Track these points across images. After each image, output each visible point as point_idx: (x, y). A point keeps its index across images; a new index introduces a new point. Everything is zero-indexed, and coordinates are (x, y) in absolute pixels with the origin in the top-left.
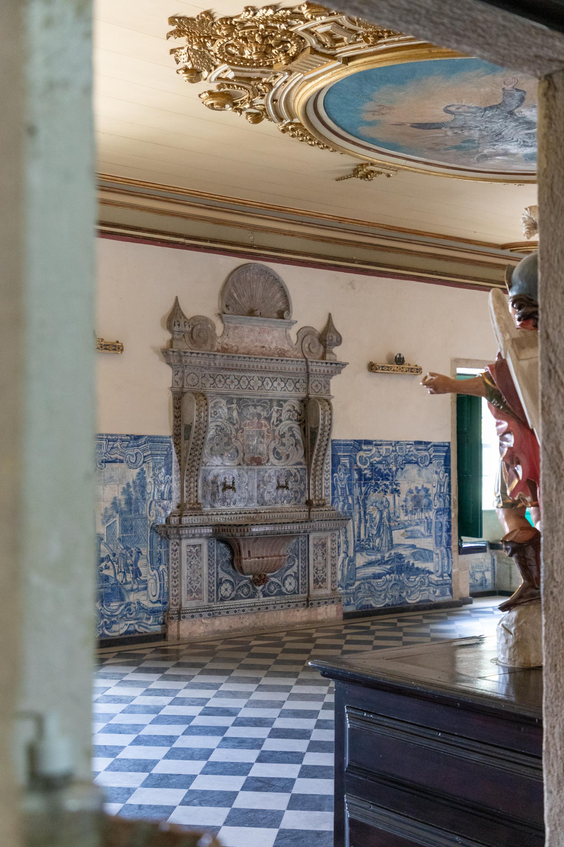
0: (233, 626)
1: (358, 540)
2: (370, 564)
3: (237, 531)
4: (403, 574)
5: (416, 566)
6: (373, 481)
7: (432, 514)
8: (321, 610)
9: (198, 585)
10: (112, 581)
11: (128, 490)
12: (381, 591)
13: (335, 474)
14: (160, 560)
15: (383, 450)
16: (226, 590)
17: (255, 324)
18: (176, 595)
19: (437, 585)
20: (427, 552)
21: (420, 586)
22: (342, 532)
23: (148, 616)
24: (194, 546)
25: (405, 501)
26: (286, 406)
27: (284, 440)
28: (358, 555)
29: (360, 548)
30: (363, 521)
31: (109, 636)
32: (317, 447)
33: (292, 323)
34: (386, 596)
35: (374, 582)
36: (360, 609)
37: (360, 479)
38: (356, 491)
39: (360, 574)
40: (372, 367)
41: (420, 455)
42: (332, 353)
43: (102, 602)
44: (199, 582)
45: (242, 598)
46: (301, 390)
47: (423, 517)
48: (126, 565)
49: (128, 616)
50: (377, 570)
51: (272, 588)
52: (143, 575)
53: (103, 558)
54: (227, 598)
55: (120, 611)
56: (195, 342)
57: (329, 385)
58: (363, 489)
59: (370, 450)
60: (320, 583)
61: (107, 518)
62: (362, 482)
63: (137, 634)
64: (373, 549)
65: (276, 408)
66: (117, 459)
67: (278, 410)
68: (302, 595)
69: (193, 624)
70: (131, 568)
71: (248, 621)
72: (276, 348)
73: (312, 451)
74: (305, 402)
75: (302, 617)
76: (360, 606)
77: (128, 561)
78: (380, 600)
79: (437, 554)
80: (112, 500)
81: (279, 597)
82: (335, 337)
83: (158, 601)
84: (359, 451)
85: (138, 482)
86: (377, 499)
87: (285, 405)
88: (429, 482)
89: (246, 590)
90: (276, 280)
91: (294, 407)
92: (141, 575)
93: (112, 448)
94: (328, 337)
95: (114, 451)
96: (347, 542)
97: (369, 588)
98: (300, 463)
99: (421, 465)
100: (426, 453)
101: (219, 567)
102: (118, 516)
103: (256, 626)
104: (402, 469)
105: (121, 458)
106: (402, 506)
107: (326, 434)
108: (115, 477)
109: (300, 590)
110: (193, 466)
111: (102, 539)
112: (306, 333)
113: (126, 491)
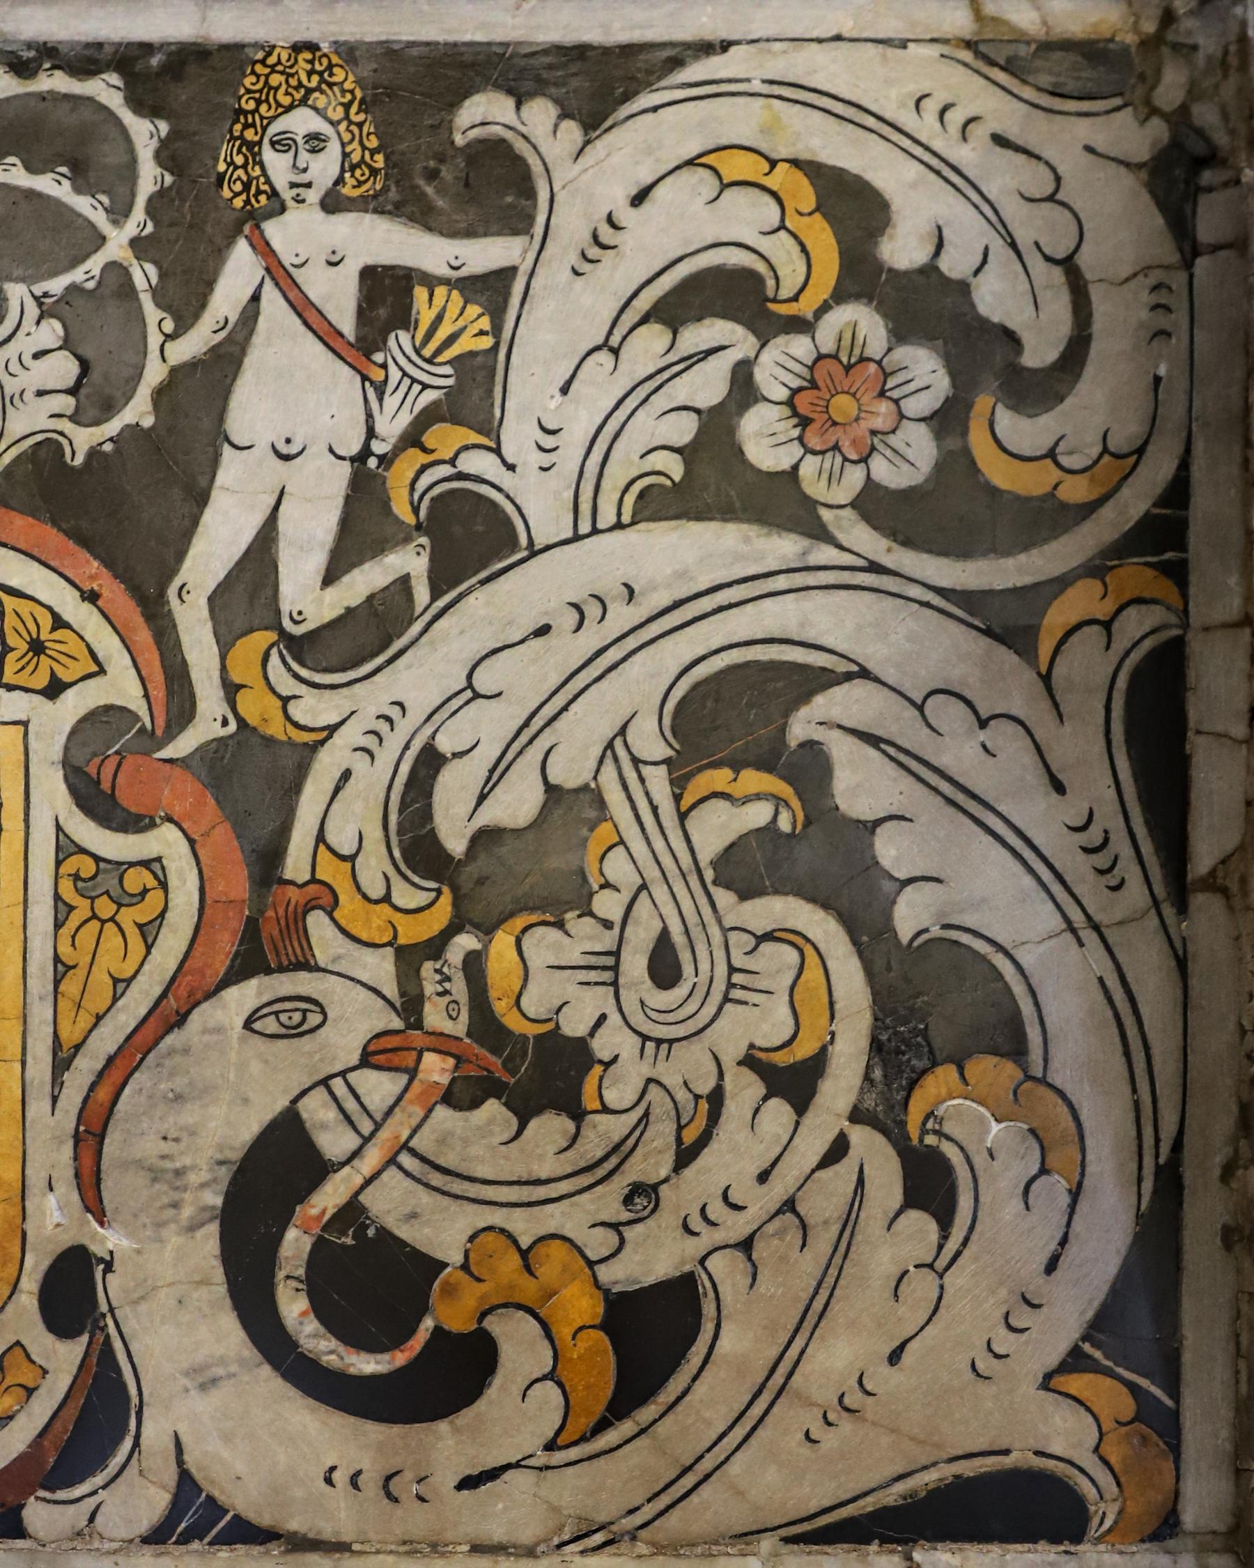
26: (629, 201)
65: (331, 247)
67: (387, 293)
87: (584, 175)
91: (851, 206)
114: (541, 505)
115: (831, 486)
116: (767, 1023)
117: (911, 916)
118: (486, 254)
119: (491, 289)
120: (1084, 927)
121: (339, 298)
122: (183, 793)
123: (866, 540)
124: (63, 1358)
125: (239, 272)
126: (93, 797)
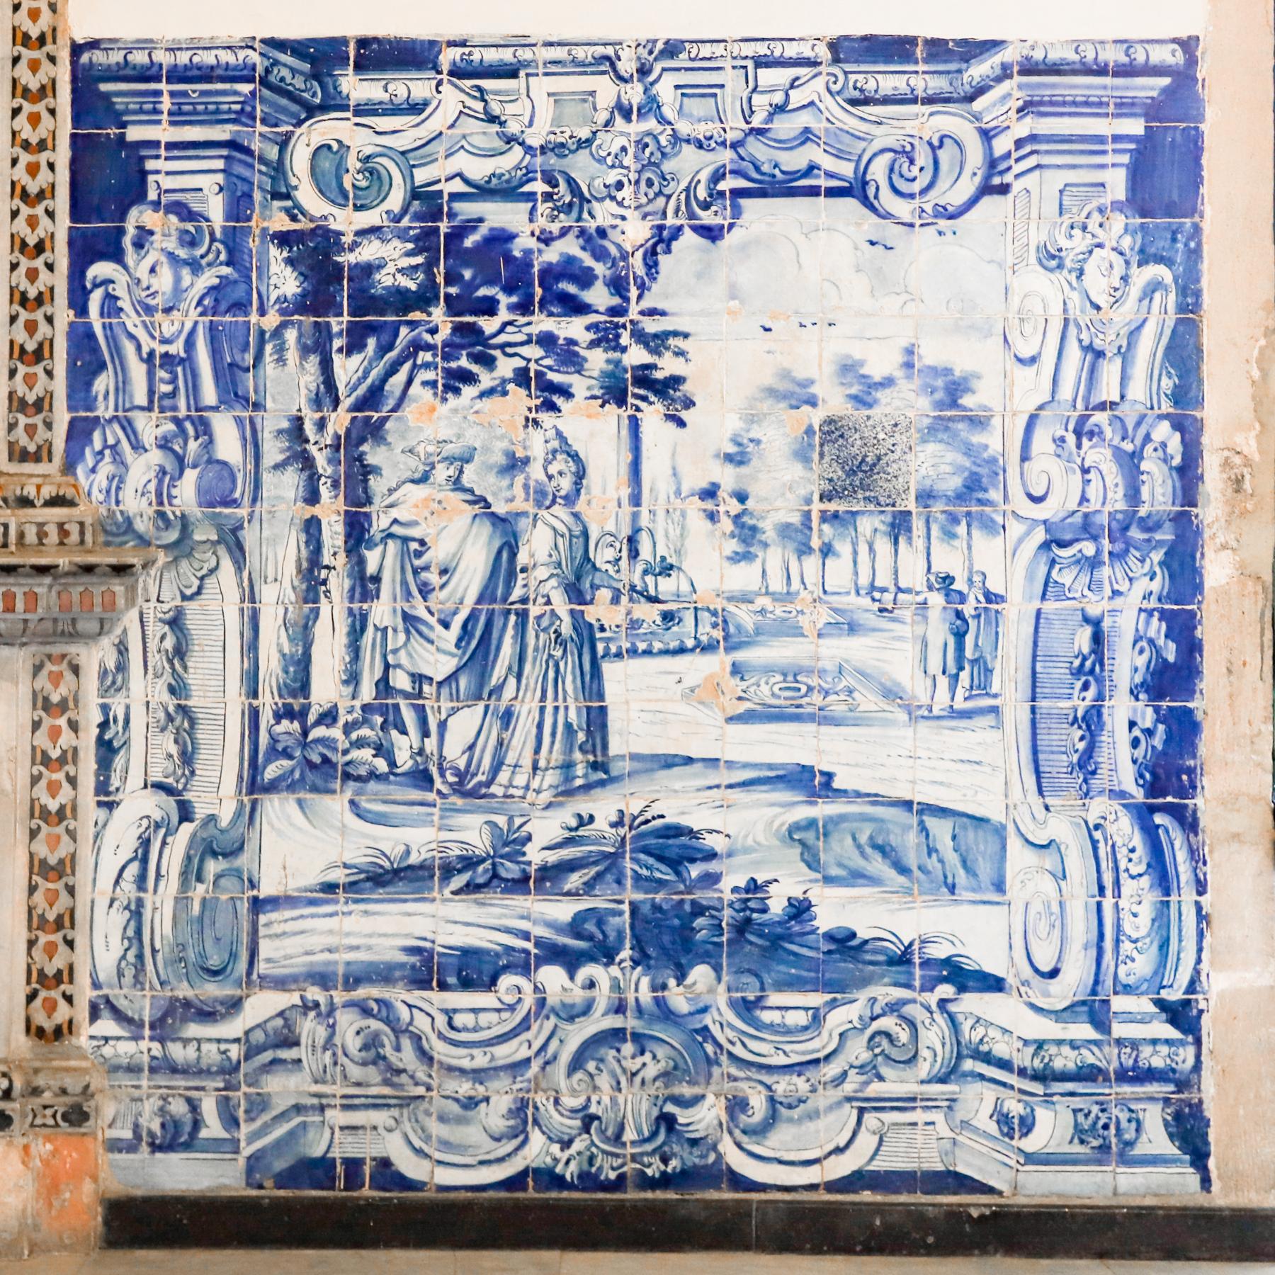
5: (826, 918)
12: (478, 1075)
13: (100, 269)
15: (536, 108)
21: (870, 1070)
28: (279, 811)
30: (338, 582)
34: (523, 1117)
35: (425, 1008)
37: (315, 301)
38: (287, 383)
39: (291, 942)
41: (885, 137)
50: (452, 921)
58: (346, 369)
59: (416, 108)
62: (338, 323)
84: (312, 111)
86: (474, 437)
96: (182, 719)
97: (372, 1043)
106: (710, 493)
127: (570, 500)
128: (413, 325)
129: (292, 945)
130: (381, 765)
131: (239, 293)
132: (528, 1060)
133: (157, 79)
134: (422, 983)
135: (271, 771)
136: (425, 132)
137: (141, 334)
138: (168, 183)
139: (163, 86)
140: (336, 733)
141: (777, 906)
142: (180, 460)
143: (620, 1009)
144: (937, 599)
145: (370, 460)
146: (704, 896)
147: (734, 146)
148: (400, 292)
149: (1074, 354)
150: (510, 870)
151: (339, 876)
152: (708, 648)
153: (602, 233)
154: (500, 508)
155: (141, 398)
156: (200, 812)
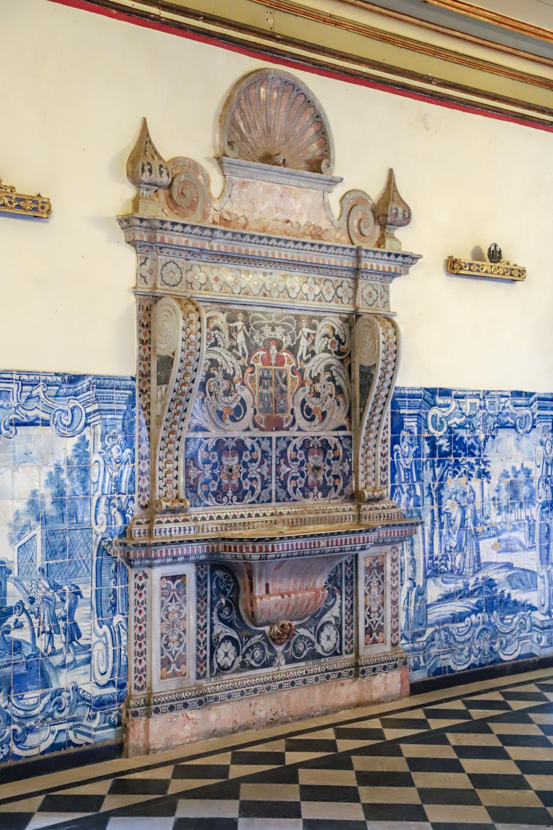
0: (239, 720)
1: (431, 558)
2: (447, 597)
3: (254, 550)
4: (495, 613)
6: (452, 458)
7: (535, 512)
8: (378, 680)
9: (181, 649)
10: (28, 651)
11: (58, 477)
12: (463, 643)
13: (396, 447)
14: (114, 605)
16: (226, 655)
17: (275, 179)
18: (142, 670)
19: (543, 629)
20: (528, 574)
21: (519, 631)
22: (406, 544)
23: (92, 713)
24: (174, 578)
25: (497, 491)
27: (318, 387)
28: (430, 582)
29: (434, 572)
30: (437, 525)
31: (19, 757)
32: (372, 399)
33: (334, 182)
34: (470, 651)
35: (453, 627)
36: (434, 674)
37: (432, 455)
38: (427, 474)
40: (453, 267)
41: (519, 414)
42: (394, 238)
43: (9, 692)
44: (181, 643)
45: (252, 668)
46: (345, 301)
47: (523, 517)
48: (54, 619)
49: (57, 715)
51: (300, 647)
52: (84, 636)
53: (11, 608)
54: (228, 668)
55: (41, 707)
56: (176, 205)
57: (387, 292)
58: (438, 471)
59: (448, 406)
60: (375, 634)
61: (19, 531)
62: (436, 459)
63: (72, 749)
64: (452, 571)
65: (306, 330)
66: (38, 419)
67: (309, 334)
68: (347, 656)
69: (173, 723)
70: (62, 624)
71: (264, 707)
72: (308, 225)
73: (363, 406)
74: (352, 320)
75: (348, 696)
76: (433, 670)
77: (58, 612)
78: (463, 657)
79: (542, 577)
80: (28, 496)
81: (310, 663)
82: (400, 210)
83: (111, 683)
84: (432, 406)
85: (75, 461)
86: (458, 488)
87: (320, 326)
88: (532, 459)
89: (258, 653)
90: (309, 102)
92: (79, 636)
93: (29, 398)
94: (388, 212)
95: (32, 403)
96: (413, 562)
97: (446, 638)
98: (342, 428)
99: (521, 431)
100: (527, 411)
101: (215, 613)
102: (39, 527)
103: (275, 718)
104: (493, 437)
105: (46, 416)
106: (494, 499)
107: (388, 376)
108: (34, 454)
109: (344, 648)
110: (173, 432)
111: (10, 572)
112: (354, 201)
113: (54, 480)
114: (317, 351)
115: (333, 351)
116: (329, 392)
117: (337, 383)
118: (314, 332)
119: (314, 334)
120: (346, 384)
121: (306, 335)
122: (298, 373)
123: (334, 355)
124: (292, 416)
125: (300, 333)
126: (293, 373)
127: (473, 502)
128: (448, 460)
129: (433, 616)
130: (446, 569)
131: (419, 453)
132: (470, 639)
133: (405, 397)
134: (453, 622)
135: (428, 573)
136: (449, 412)
137: (403, 463)
138: (408, 424)
139: (406, 399)
140: (438, 562)
141: (506, 595)
142: (410, 495)
143: (484, 623)
144: (527, 522)
145: (442, 494)
146: (495, 594)
147: (497, 416)
148: (446, 451)
149: (545, 464)
150: (467, 593)
151: (440, 597)
152: (494, 536)
153: (477, 437)
154: (462, 505)
155: (403, 480)
156: (417, 584)
